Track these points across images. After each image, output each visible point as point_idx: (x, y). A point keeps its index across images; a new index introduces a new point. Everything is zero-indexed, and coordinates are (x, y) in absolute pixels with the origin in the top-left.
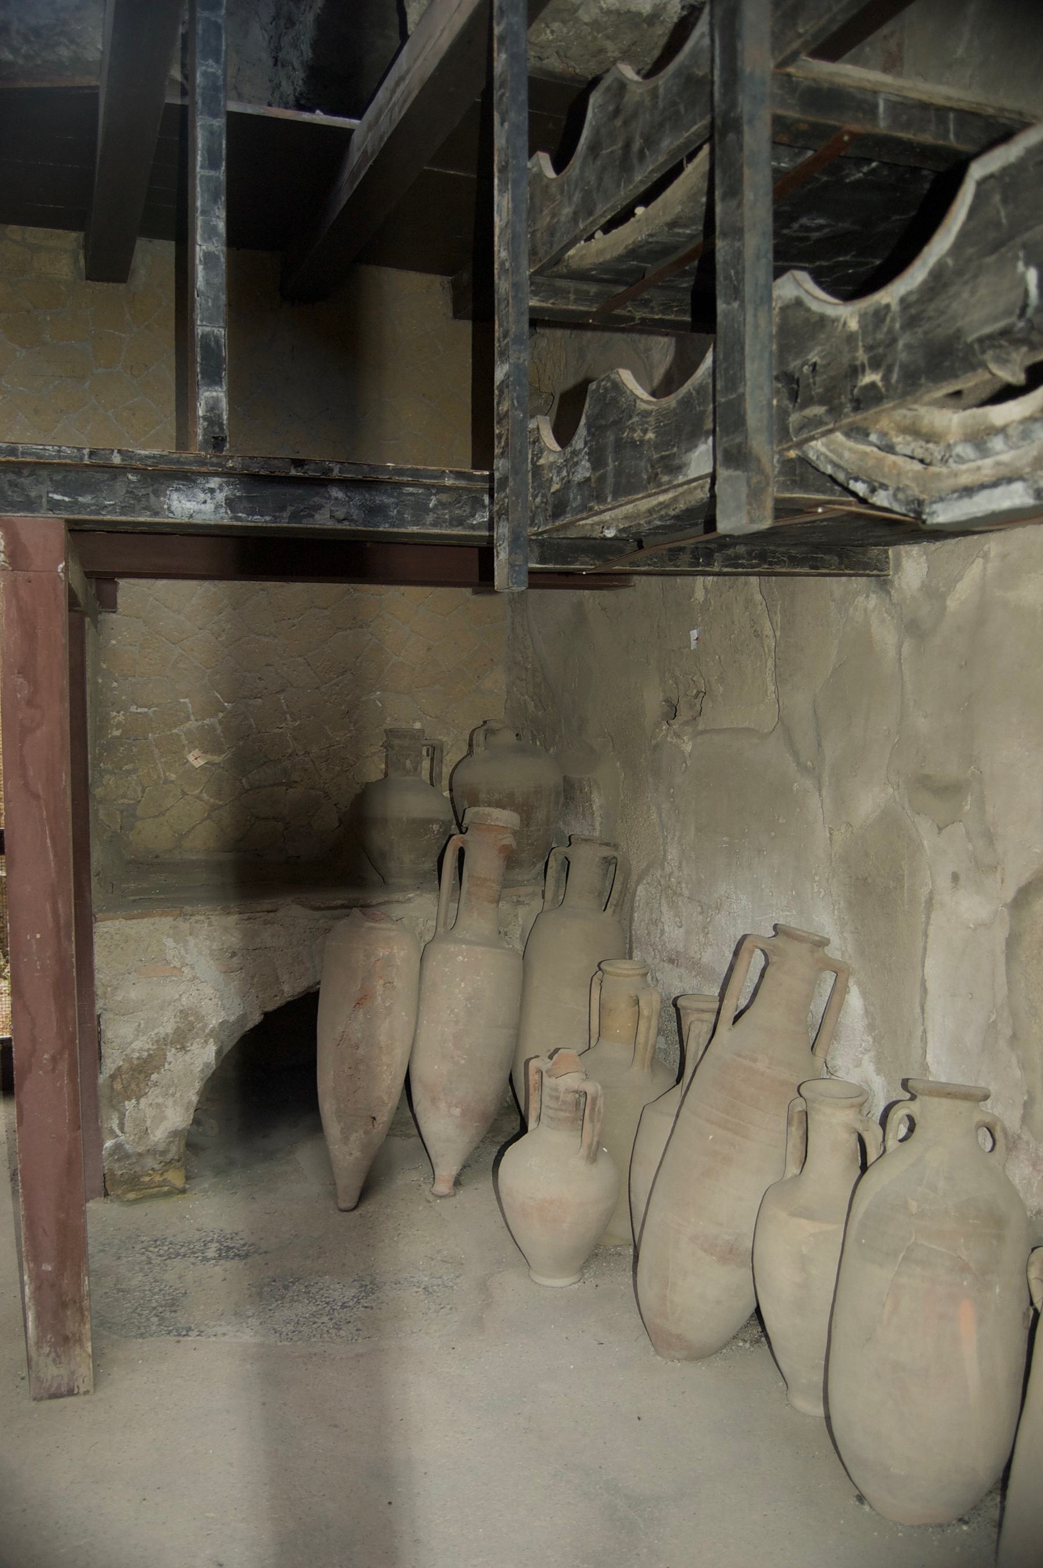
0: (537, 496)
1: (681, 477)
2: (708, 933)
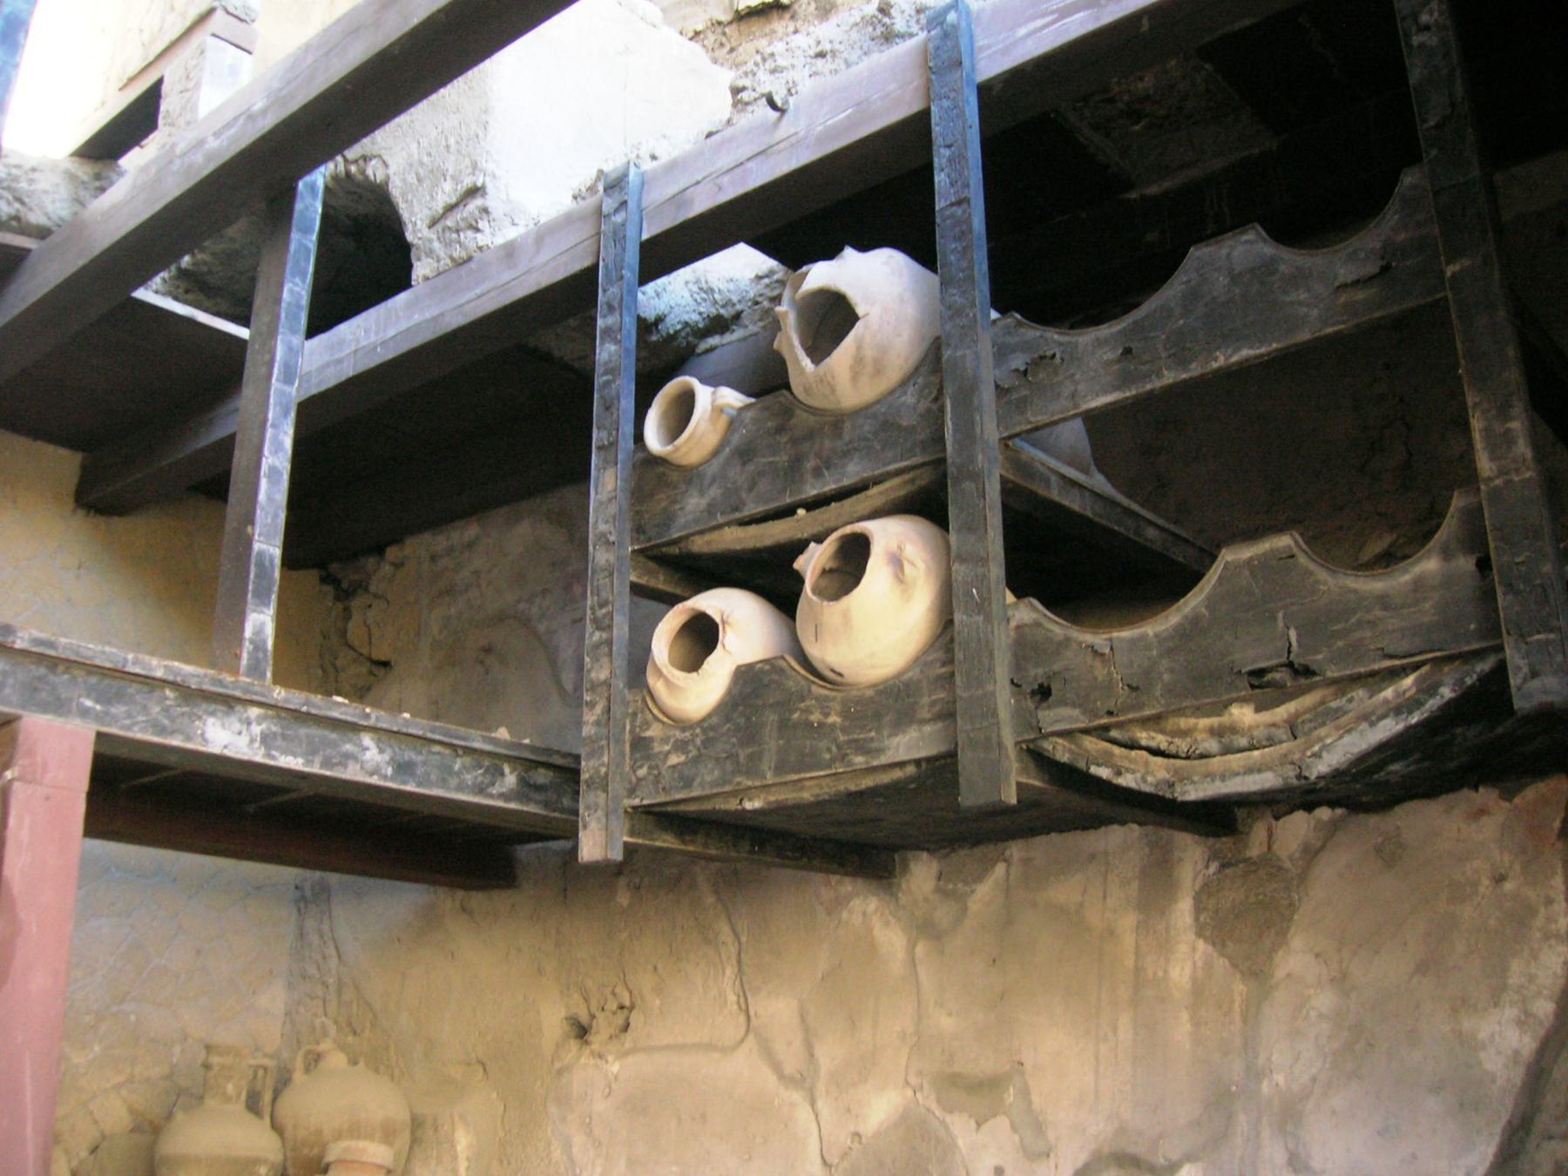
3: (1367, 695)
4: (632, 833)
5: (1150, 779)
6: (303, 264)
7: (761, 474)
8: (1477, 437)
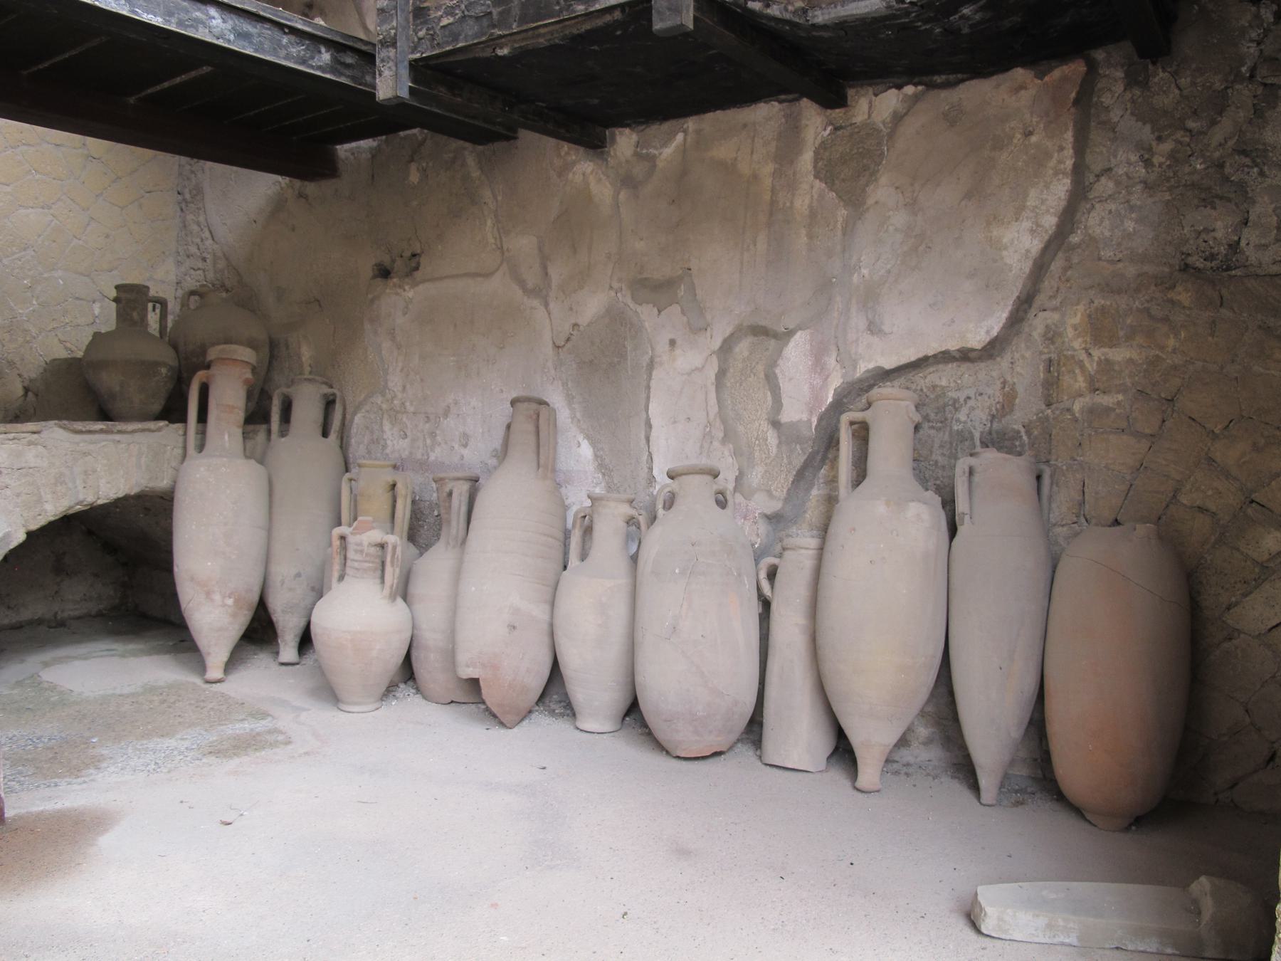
2: (436, 436)
4: (412, 82)
5: (790, 8)
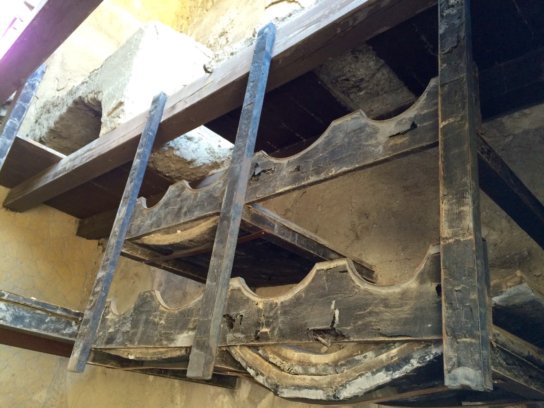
0: (101, 331)
1: (172, 344)
3: (374, 356)
6: (20, 113)
7: (168, 213)
8: (443, 214)
